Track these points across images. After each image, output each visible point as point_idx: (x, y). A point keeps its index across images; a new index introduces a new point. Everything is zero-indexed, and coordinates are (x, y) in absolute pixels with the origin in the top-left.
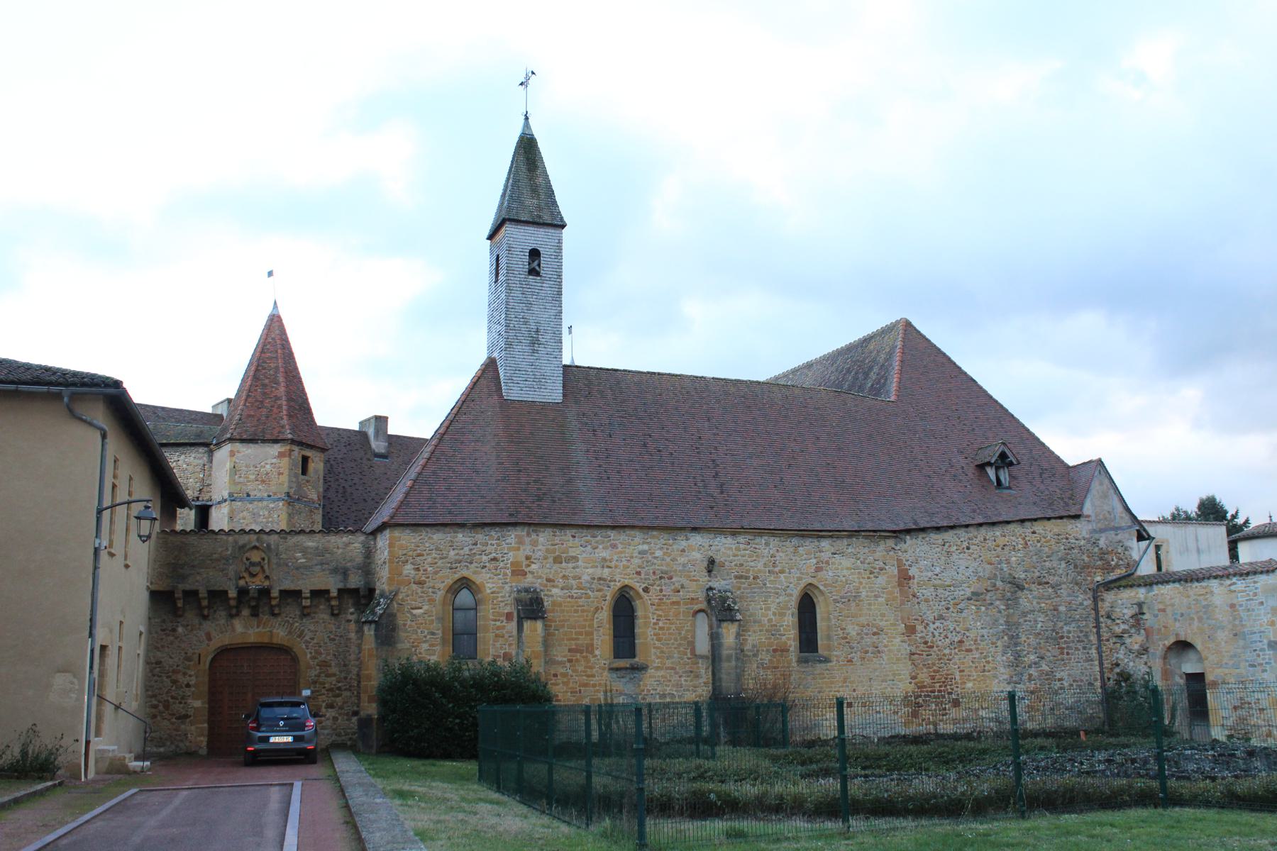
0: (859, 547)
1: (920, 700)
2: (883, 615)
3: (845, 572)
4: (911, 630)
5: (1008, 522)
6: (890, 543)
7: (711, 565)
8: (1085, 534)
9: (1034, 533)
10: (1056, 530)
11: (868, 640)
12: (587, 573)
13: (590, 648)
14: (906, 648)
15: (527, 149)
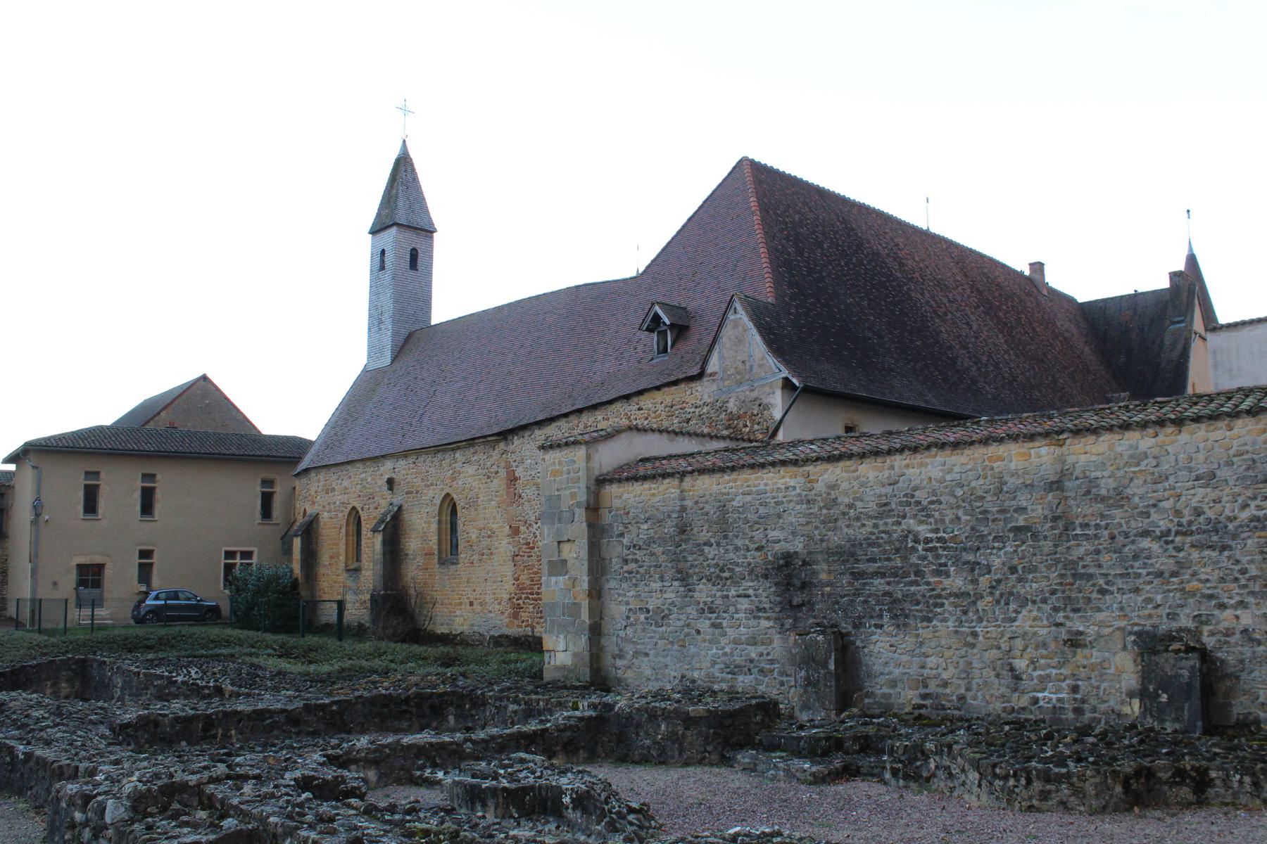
0: (479, 455)
1: (520, 602)
2: (494, 518)
3: (470, 480)
4: (515, 531)
5: (610, 402)
6: (502, 445)
7: (390, 482)
8: (706, 399)
9: (640, 409)
10: (668, 400)
11: (485, 543)
12: (339, 498)
13: (338, 554)
14: (511, 549)
15: (403, 171)
